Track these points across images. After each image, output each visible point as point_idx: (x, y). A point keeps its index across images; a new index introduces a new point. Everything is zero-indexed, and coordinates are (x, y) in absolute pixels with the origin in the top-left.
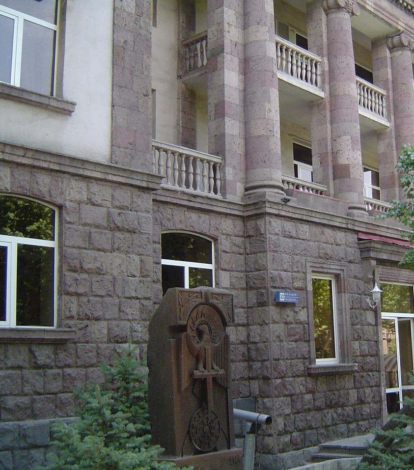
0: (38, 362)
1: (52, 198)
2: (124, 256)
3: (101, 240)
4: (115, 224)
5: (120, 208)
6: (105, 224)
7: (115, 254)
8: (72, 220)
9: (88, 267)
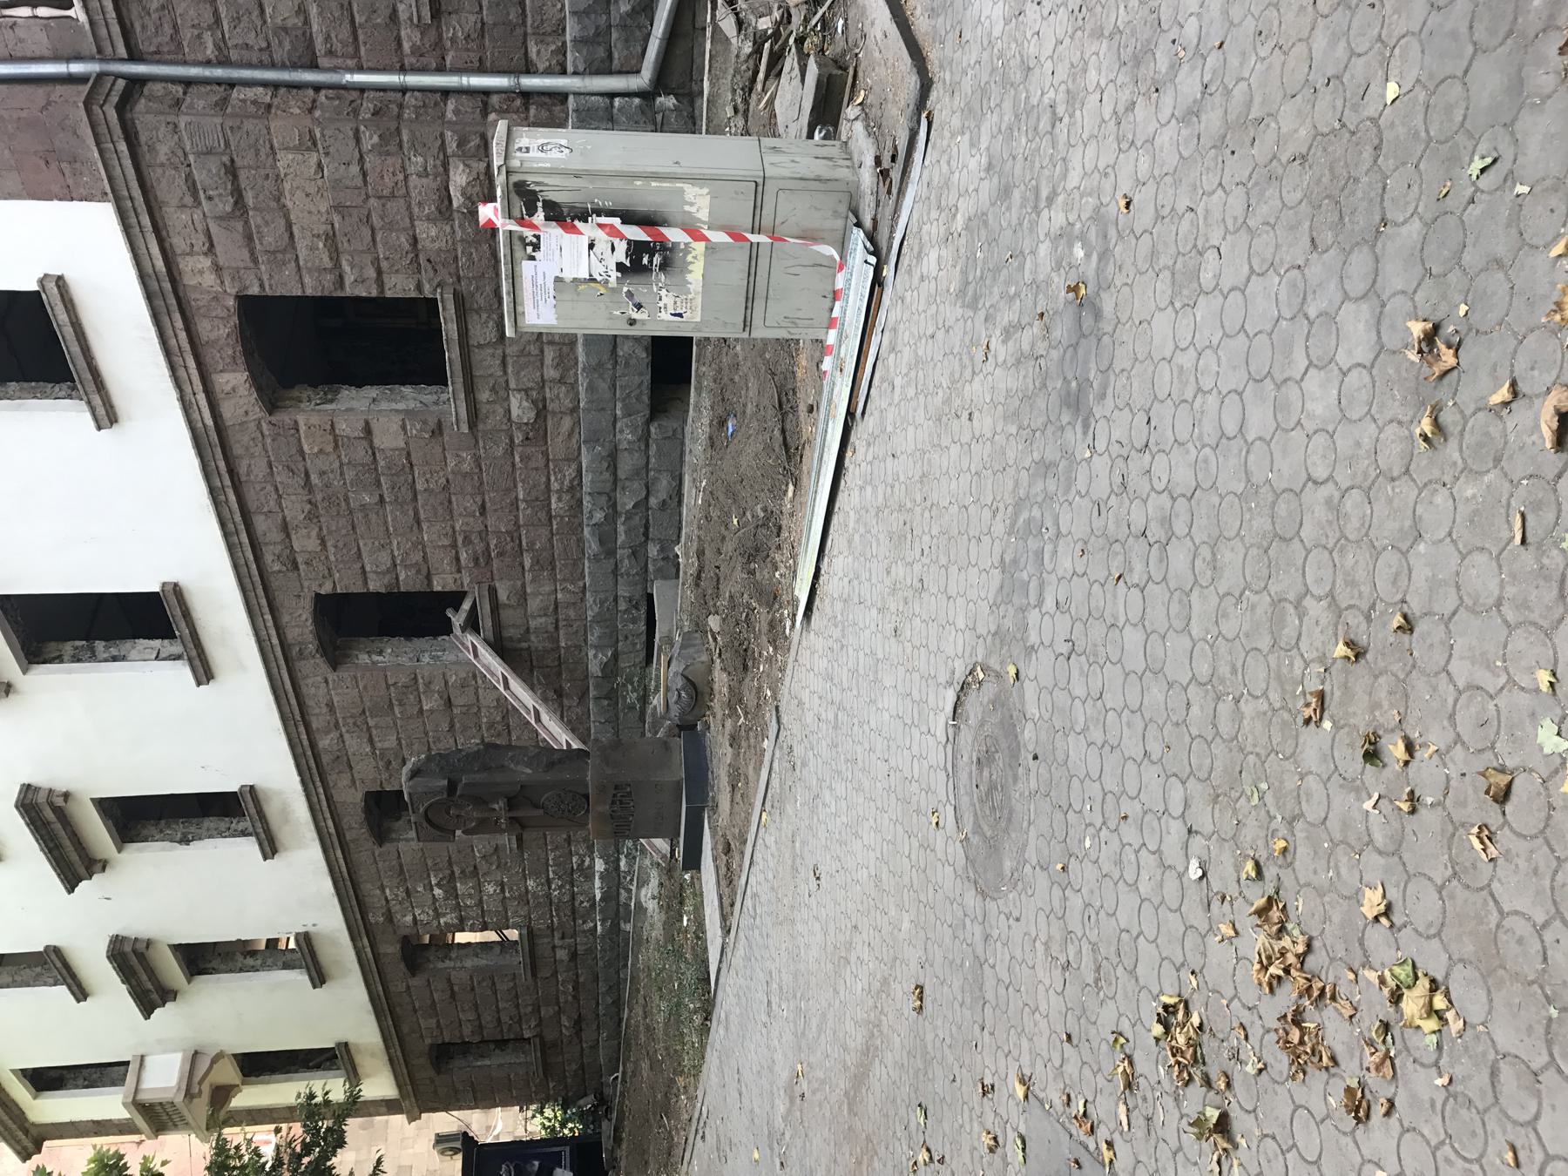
7: (289, 204)
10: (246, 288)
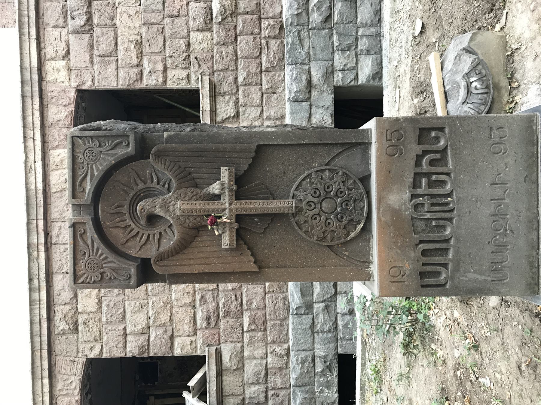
0: (232, 115)
1: (71, 102)
2: (119, 11)
3: (105, 42)
4: (85, 24)
6: (86, 37)
7: (118, 23)
8: (90, 79)
9: (136, 59)
10: (83, 83)
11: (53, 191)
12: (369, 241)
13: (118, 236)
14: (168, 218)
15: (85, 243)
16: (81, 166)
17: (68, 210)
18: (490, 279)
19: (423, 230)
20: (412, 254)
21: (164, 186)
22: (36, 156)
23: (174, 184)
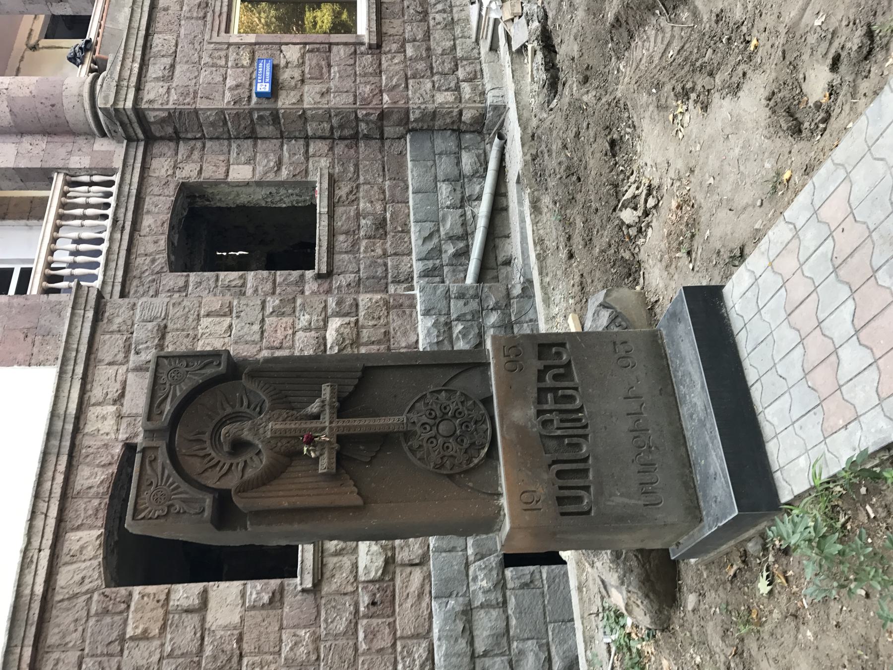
5: (127, 352)
11: (58, 598)
12: (496, 469)
13: (194, 465)
14: (257, 442)
15: (154, 470)
16: (162, 387)
17: (76, 630)
18: (641, 503)
19: (556, 451)
20: (545, 476)
21: (255, 409)
22: (44, 541)
23: (267, 405)
